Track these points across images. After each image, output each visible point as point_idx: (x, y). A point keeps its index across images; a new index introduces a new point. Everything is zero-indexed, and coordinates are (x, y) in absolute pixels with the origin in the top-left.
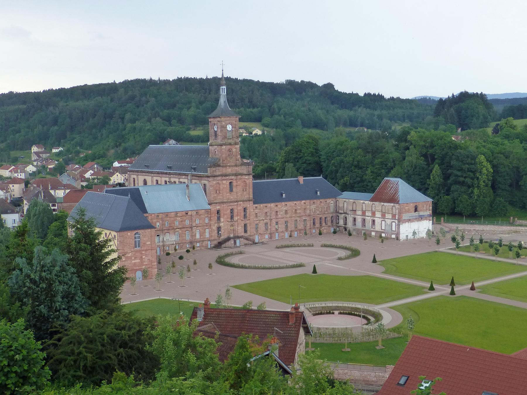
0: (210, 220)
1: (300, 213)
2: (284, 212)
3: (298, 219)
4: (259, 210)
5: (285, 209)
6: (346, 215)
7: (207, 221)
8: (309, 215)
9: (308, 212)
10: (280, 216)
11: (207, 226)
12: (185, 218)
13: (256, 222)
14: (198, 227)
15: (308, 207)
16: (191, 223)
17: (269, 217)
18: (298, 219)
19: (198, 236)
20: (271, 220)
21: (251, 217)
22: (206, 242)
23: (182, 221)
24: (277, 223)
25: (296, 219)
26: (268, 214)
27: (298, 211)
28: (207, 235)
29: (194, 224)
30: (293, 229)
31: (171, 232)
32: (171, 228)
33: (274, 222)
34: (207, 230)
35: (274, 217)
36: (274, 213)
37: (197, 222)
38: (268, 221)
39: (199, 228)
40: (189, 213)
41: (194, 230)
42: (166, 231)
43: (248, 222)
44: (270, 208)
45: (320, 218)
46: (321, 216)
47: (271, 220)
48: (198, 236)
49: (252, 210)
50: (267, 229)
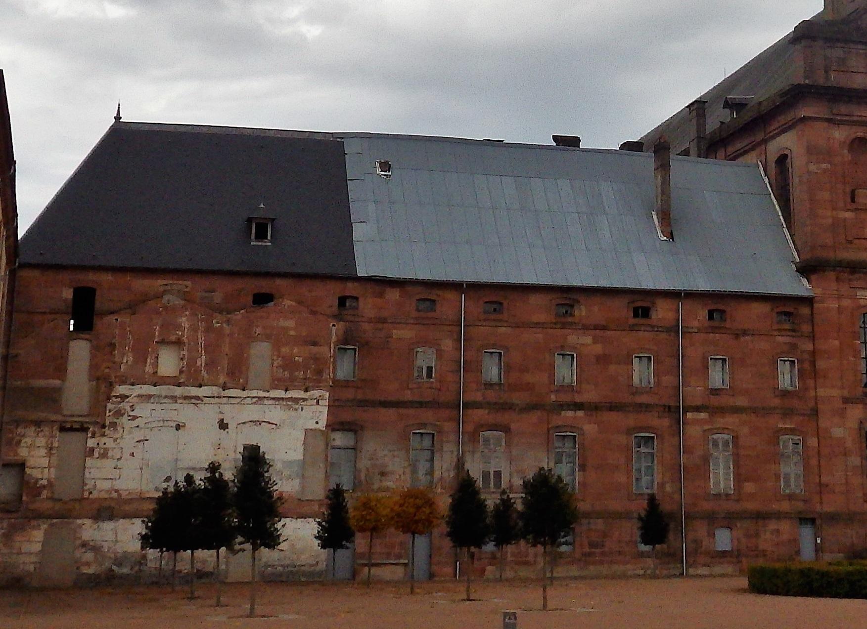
0: (809, 371)
7: (786, 378)
11: (787, 413)
12: (628, 340)
14: (722, 410)
16: (667, 380)
19: (721, 477)
22: (785, 527)
23: (603, 360)
28: (791, 472)
29: (694, 392)
31: (522, 423)
32: (519, 398)
34: (787, 443)
37: (717, 377)
39: (730, 420)
40: (662, 312)
41: (694, 431)
42: (480, 415)
48: (721, 477)
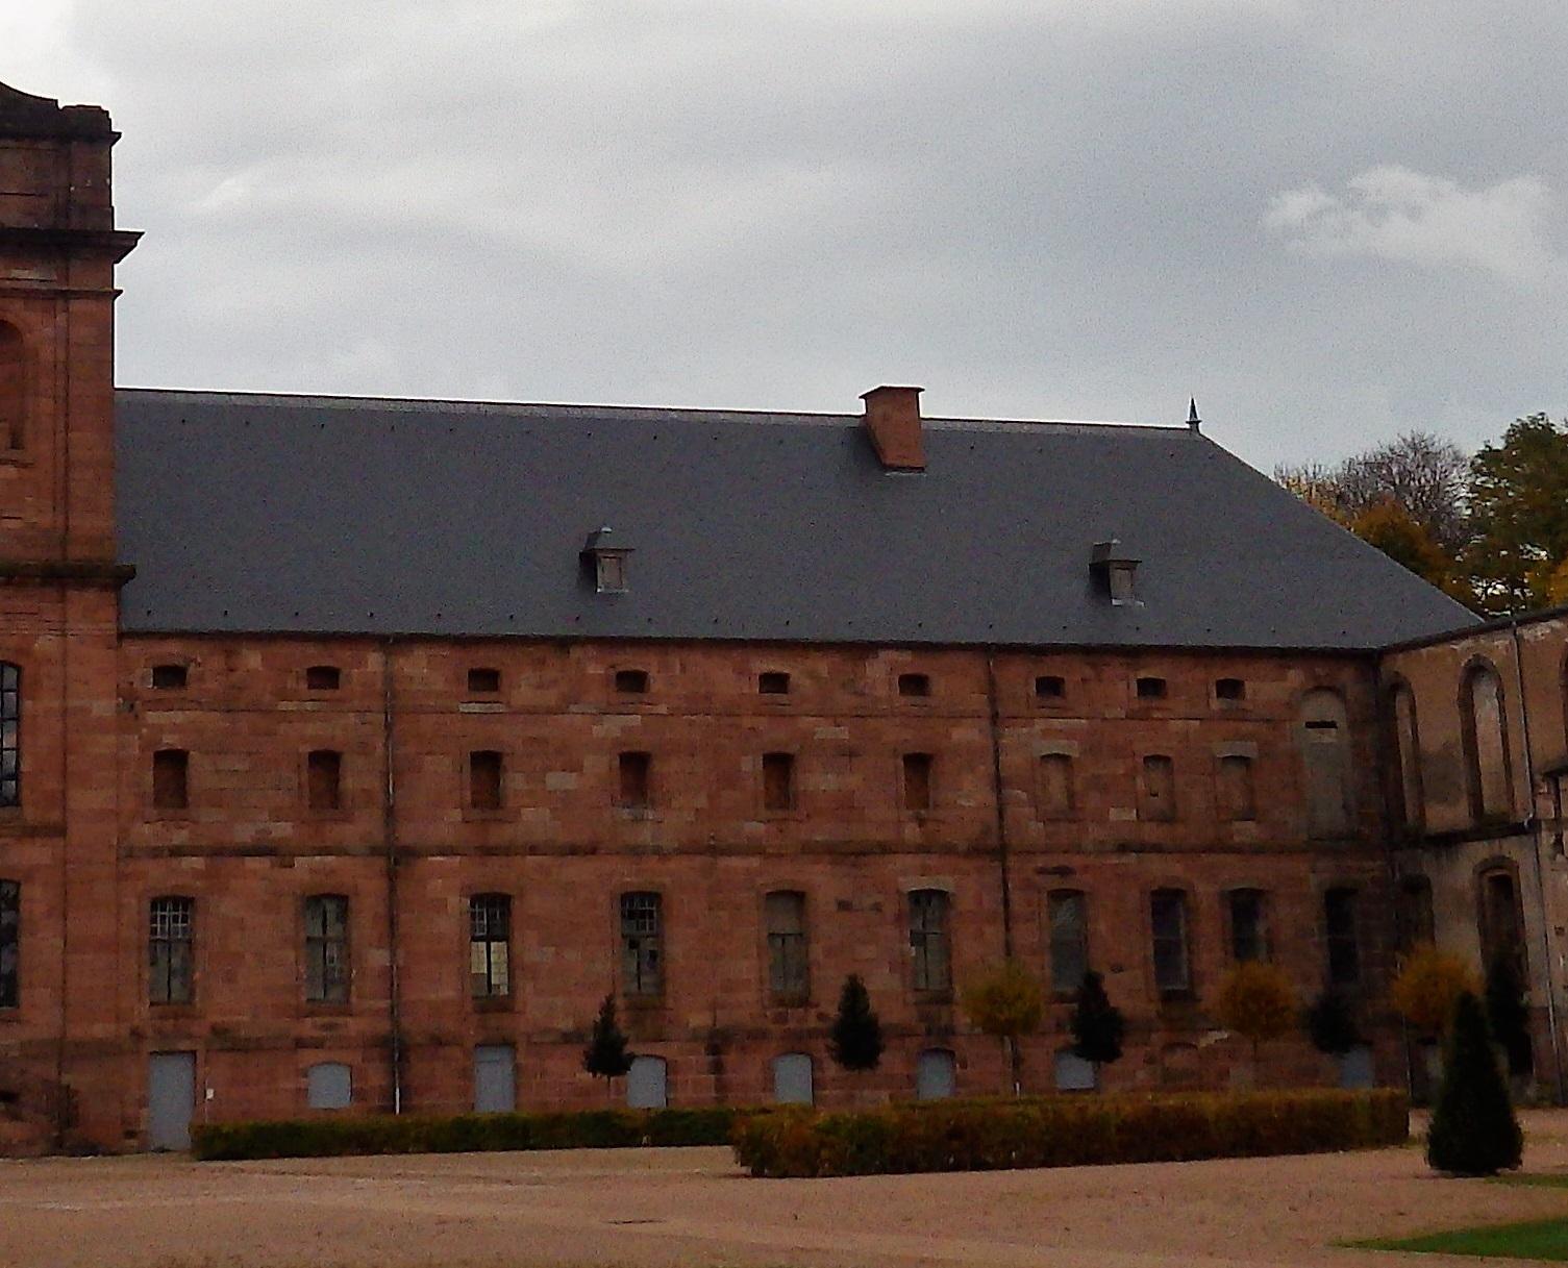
1: (845, 807)
2: (599, 766)
3: (824, 883)
4: (214, 721)
5: (612, 727)
6: (1512, 849)
8: (994, 850)
9: (966, 797)
10: (534, 821)
13: (160, 876)
15: (967, 734)
17: (363, 827)
18: (824, 883)
20: (397, 859)
21: (85, 800)
24: (493, 913)
25: (786, 874)
26: (357, 778)
27: (818, 781)
30: (746, 1007)
33: (445, 887)
35: (449, 824)
36: (441, 773)
38: (363, 879)
43: (36, 854)
44: (393, 704)
45: (1167, 903)
46: (1163, 870)
47: (397, 859)
49: (103, 707)
50: (332, 980)
